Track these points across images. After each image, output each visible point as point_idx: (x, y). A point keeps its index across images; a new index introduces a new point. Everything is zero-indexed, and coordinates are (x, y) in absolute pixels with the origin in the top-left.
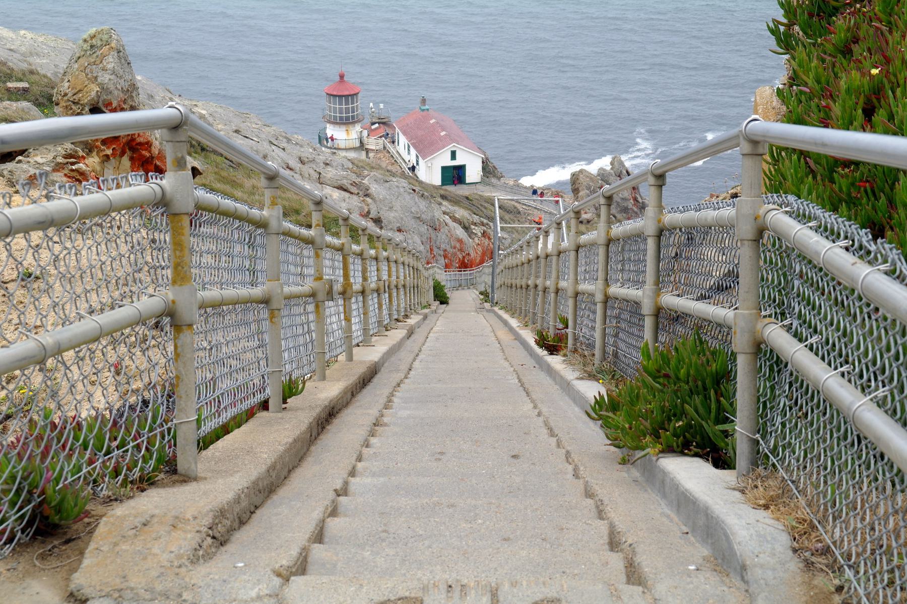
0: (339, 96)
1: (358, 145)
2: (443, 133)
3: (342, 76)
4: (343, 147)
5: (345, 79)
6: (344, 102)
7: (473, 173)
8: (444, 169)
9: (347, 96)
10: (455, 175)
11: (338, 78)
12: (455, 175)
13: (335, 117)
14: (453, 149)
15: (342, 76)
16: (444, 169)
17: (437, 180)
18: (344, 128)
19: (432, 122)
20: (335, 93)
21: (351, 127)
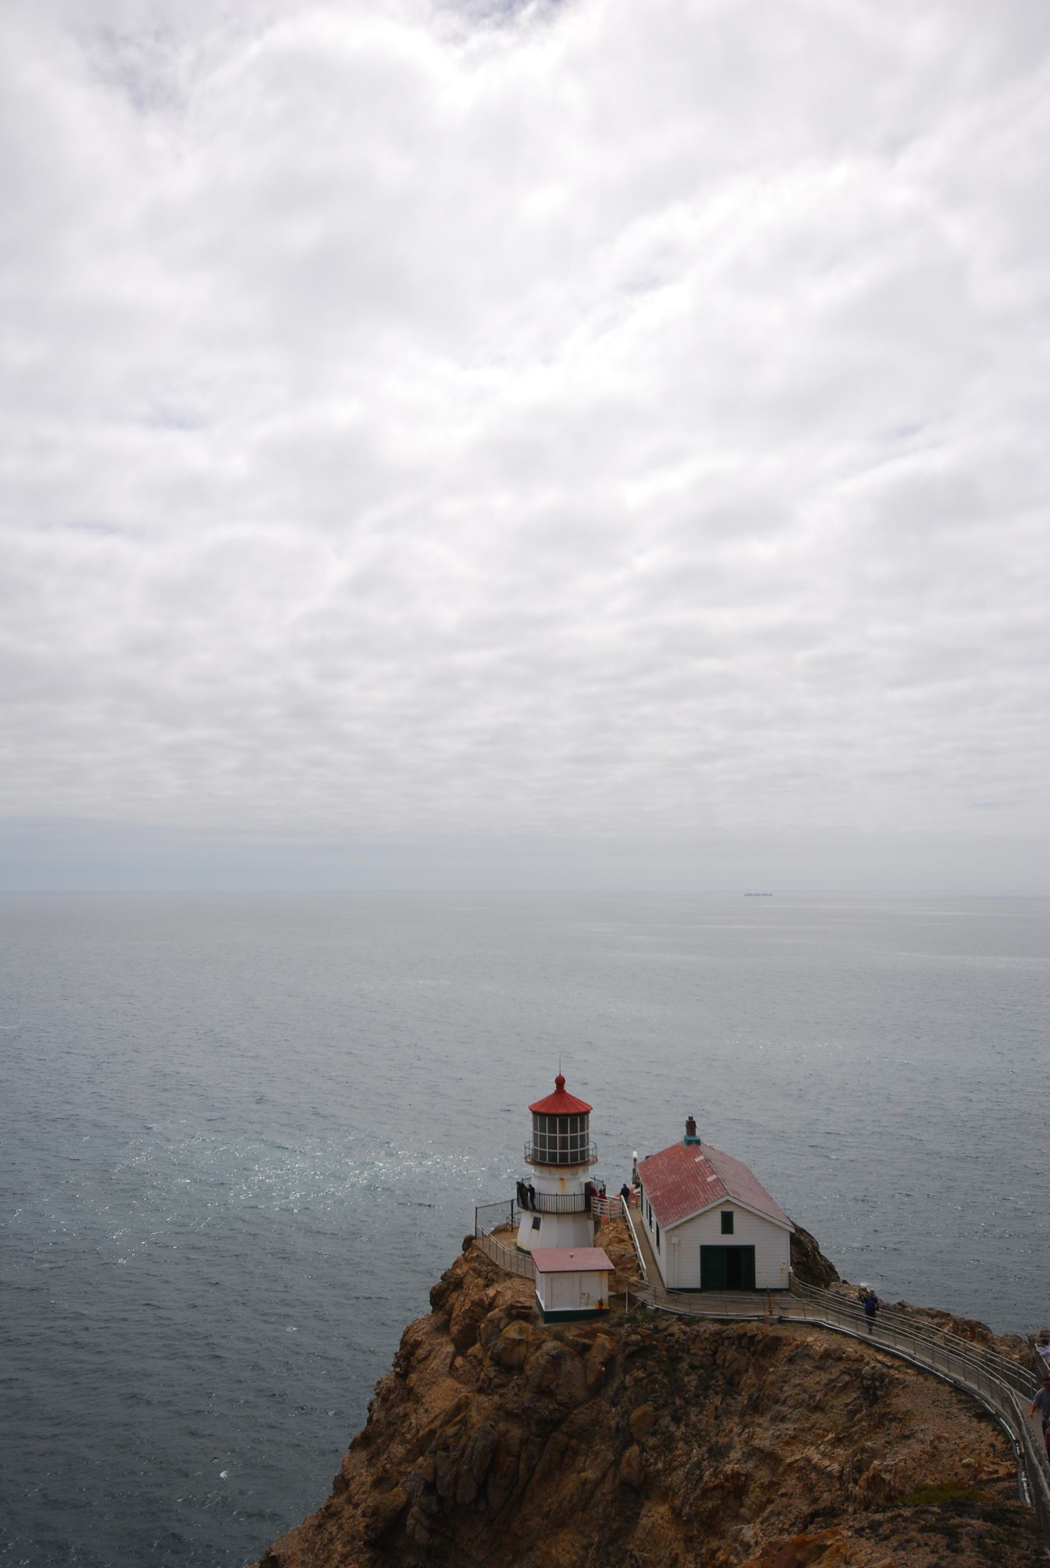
0: (553, 1117)
1: (580, 1206)
2: (709, 1179)
3: (560, 1082)
4: (554, 1210)
5: (568, 1088)
6: (561, 1127)
7: (773, 1266)
8: (708, 1253)
9: (563, 1117)
10: (728, 1268)
11: (552, 1088)
12: (728, 1268)
13: (553, 1156)
14: (728, 1209)
15: (560, 1082)
16: (708, 1253)
17: (691, 1275)
18: (558, 1173)
19: (697, 1160)
20: (543, 1110)
21: (566, 1173)
